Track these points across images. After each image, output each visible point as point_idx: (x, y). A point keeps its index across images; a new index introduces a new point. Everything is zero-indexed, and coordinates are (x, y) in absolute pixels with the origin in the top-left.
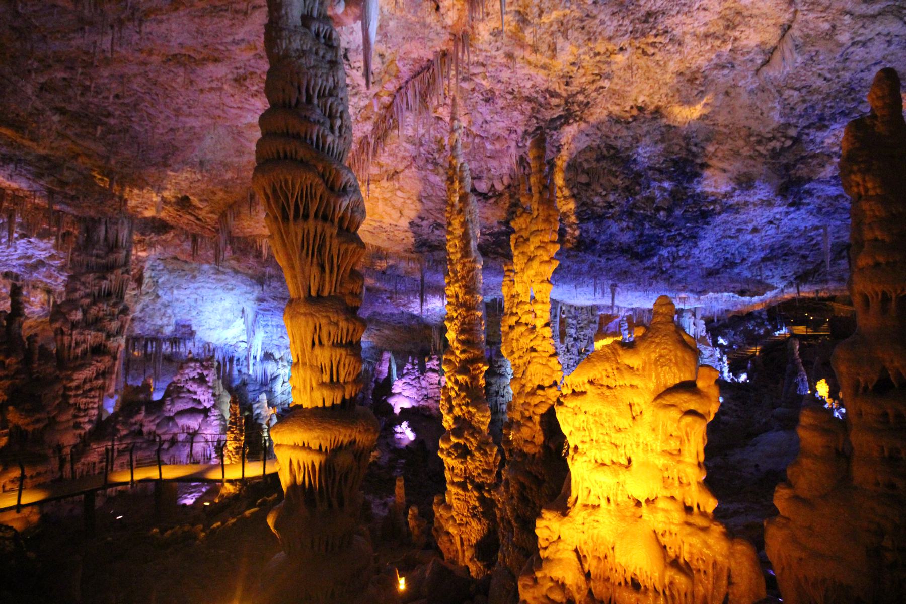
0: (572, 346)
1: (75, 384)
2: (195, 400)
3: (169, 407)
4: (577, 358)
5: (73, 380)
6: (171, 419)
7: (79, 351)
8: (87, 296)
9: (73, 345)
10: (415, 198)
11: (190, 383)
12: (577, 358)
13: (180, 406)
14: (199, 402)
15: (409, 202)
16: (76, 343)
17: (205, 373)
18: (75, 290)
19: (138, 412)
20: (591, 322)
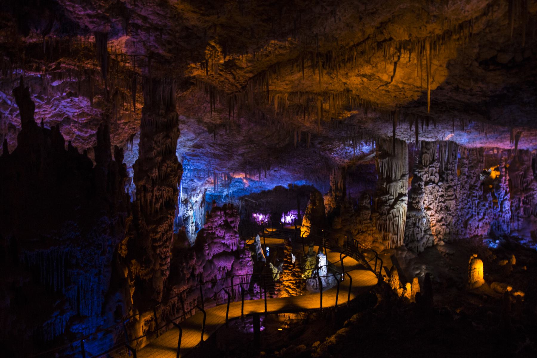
0: (466, 183)
1: (159, 236)
2: (224, 244)
3: (207, 252)
4: (468, 192)
5: (157, 233)
6: (211, 262)
7: (158, 206)
8: (159, 153)
9: (154, 200)
10: (445, 65)
11: (219, 229)
12: (468, 192)
13: (216, 250)
14: (228, 247)
15: (440, 68)
16: (156, 199)
17: (229, 220)
18: (151, 149)
19: (191, 258)
20: (479, 161)
